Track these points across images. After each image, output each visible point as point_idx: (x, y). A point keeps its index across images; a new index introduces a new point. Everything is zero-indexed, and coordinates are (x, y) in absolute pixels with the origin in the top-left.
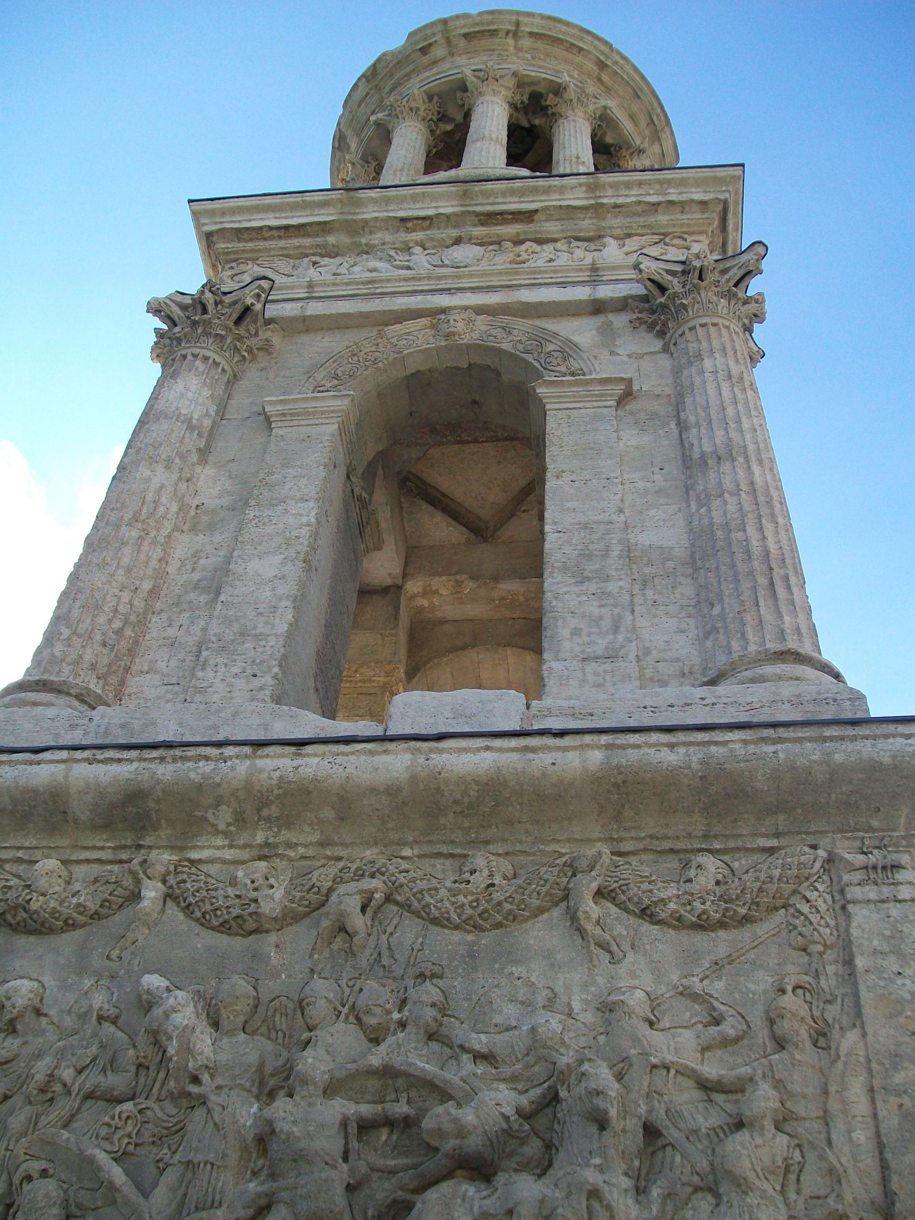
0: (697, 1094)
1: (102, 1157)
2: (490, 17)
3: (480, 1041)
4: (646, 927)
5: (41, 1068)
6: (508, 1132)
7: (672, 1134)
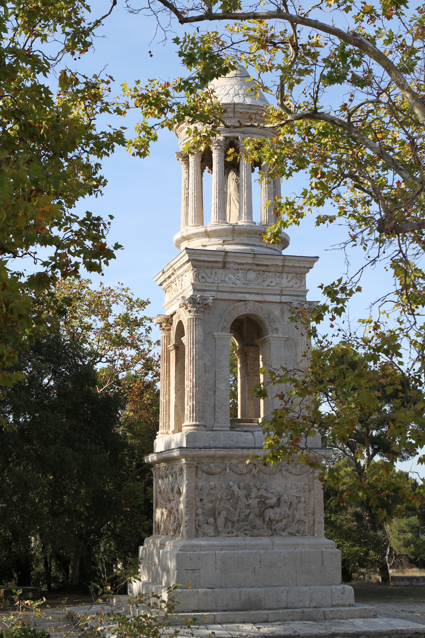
2: (249, 107)
3: (272, 491)
4: (291, 475)
7: (293, 503)
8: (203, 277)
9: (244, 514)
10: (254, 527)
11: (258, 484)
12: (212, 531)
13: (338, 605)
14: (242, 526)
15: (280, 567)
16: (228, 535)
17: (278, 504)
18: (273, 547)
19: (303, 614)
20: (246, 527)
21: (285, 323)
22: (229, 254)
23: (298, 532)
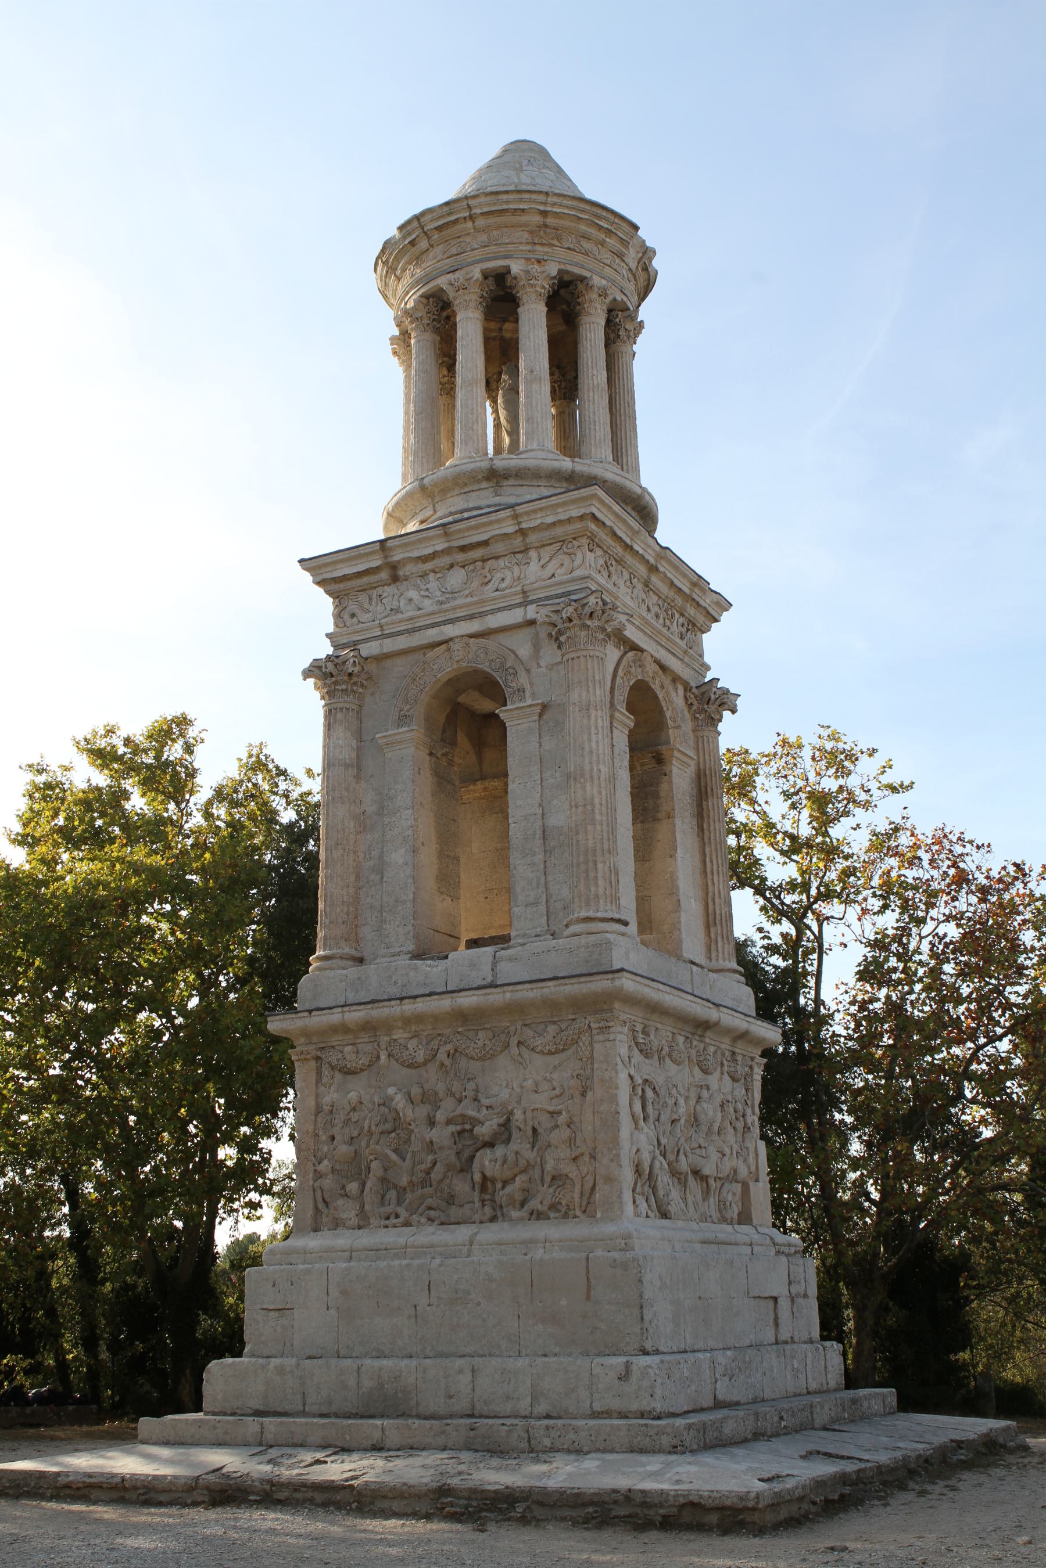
0: (548, 1115)
1: (389, 1152)
2: (446, 209)
4: (534, 1055)
5: (366, 1125)
6: (496, 1134)
7: (540, 1130)
8: (353, 615)
9: (423, 1167)
10: (451, 1200)
11: (456, 1087)
12: (352, 1214)
13: (608, 1414)
14: (423, 1197)
15: (479, 1304)
16: (383, 1222)
17: (505, 1132)
18: (469, 1251)
19: (472, 1433)
20: (429, 1202)
21: (544, 670)
22: (389, 544)
23: (553, 1207)
